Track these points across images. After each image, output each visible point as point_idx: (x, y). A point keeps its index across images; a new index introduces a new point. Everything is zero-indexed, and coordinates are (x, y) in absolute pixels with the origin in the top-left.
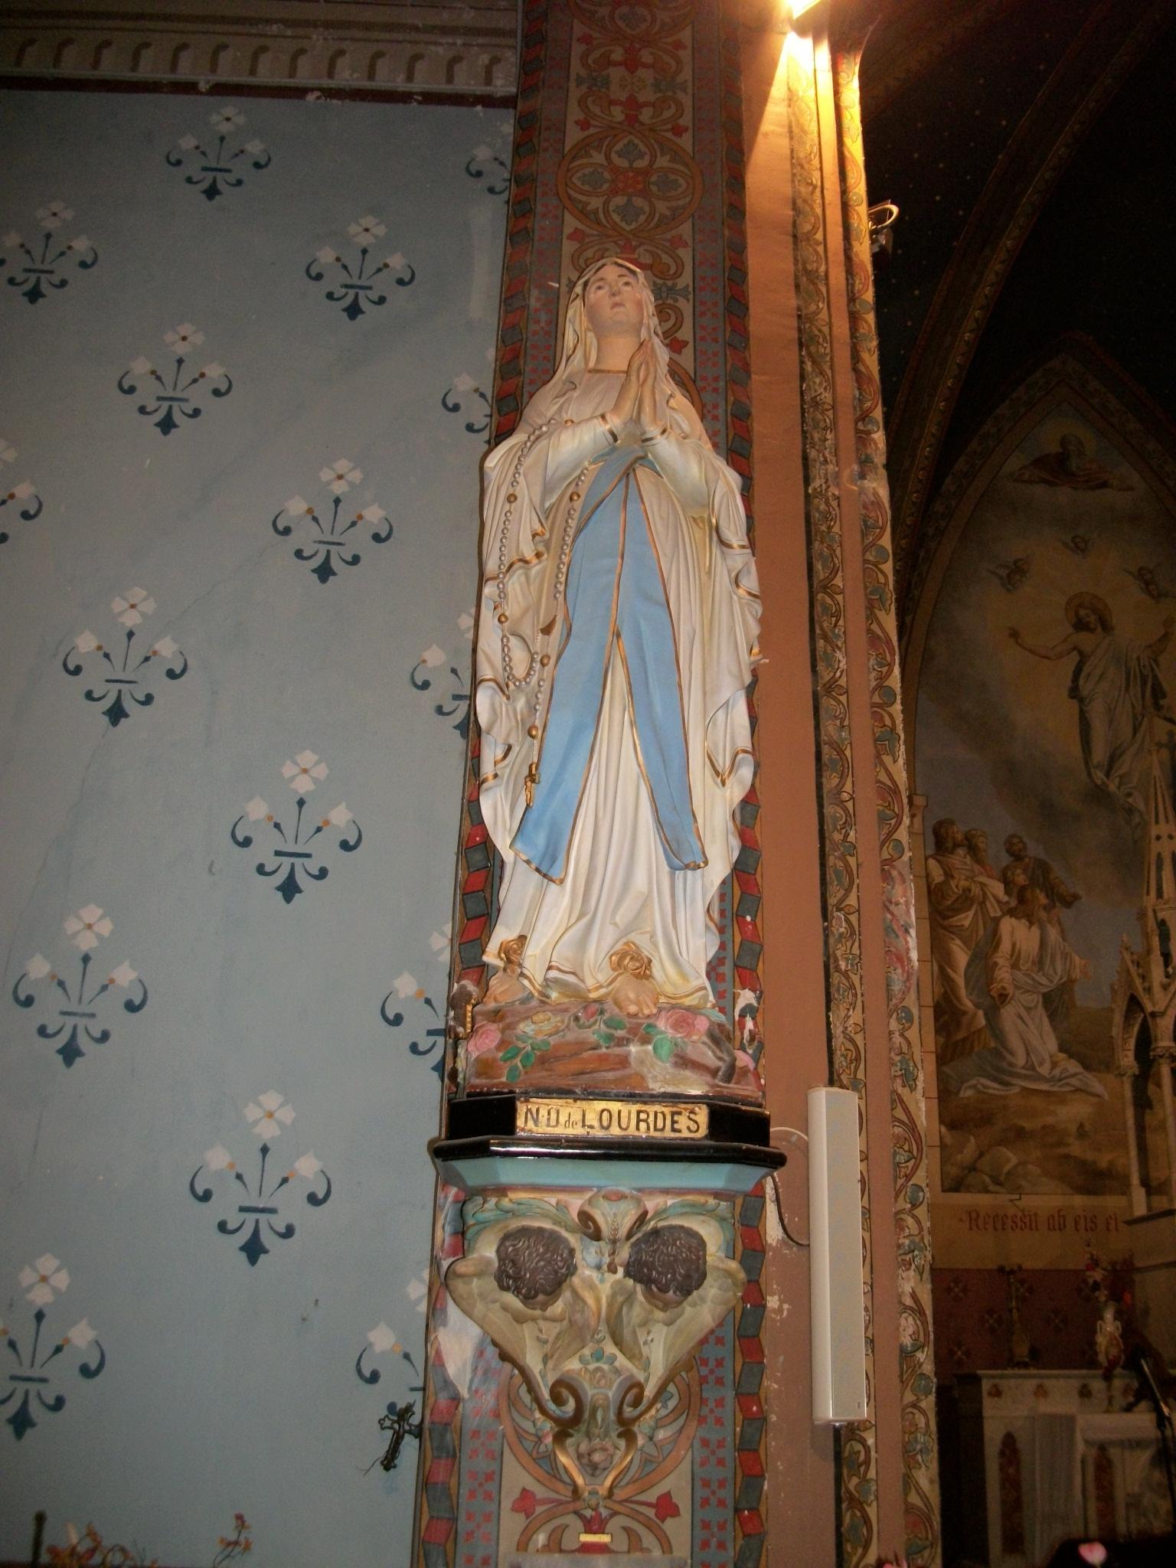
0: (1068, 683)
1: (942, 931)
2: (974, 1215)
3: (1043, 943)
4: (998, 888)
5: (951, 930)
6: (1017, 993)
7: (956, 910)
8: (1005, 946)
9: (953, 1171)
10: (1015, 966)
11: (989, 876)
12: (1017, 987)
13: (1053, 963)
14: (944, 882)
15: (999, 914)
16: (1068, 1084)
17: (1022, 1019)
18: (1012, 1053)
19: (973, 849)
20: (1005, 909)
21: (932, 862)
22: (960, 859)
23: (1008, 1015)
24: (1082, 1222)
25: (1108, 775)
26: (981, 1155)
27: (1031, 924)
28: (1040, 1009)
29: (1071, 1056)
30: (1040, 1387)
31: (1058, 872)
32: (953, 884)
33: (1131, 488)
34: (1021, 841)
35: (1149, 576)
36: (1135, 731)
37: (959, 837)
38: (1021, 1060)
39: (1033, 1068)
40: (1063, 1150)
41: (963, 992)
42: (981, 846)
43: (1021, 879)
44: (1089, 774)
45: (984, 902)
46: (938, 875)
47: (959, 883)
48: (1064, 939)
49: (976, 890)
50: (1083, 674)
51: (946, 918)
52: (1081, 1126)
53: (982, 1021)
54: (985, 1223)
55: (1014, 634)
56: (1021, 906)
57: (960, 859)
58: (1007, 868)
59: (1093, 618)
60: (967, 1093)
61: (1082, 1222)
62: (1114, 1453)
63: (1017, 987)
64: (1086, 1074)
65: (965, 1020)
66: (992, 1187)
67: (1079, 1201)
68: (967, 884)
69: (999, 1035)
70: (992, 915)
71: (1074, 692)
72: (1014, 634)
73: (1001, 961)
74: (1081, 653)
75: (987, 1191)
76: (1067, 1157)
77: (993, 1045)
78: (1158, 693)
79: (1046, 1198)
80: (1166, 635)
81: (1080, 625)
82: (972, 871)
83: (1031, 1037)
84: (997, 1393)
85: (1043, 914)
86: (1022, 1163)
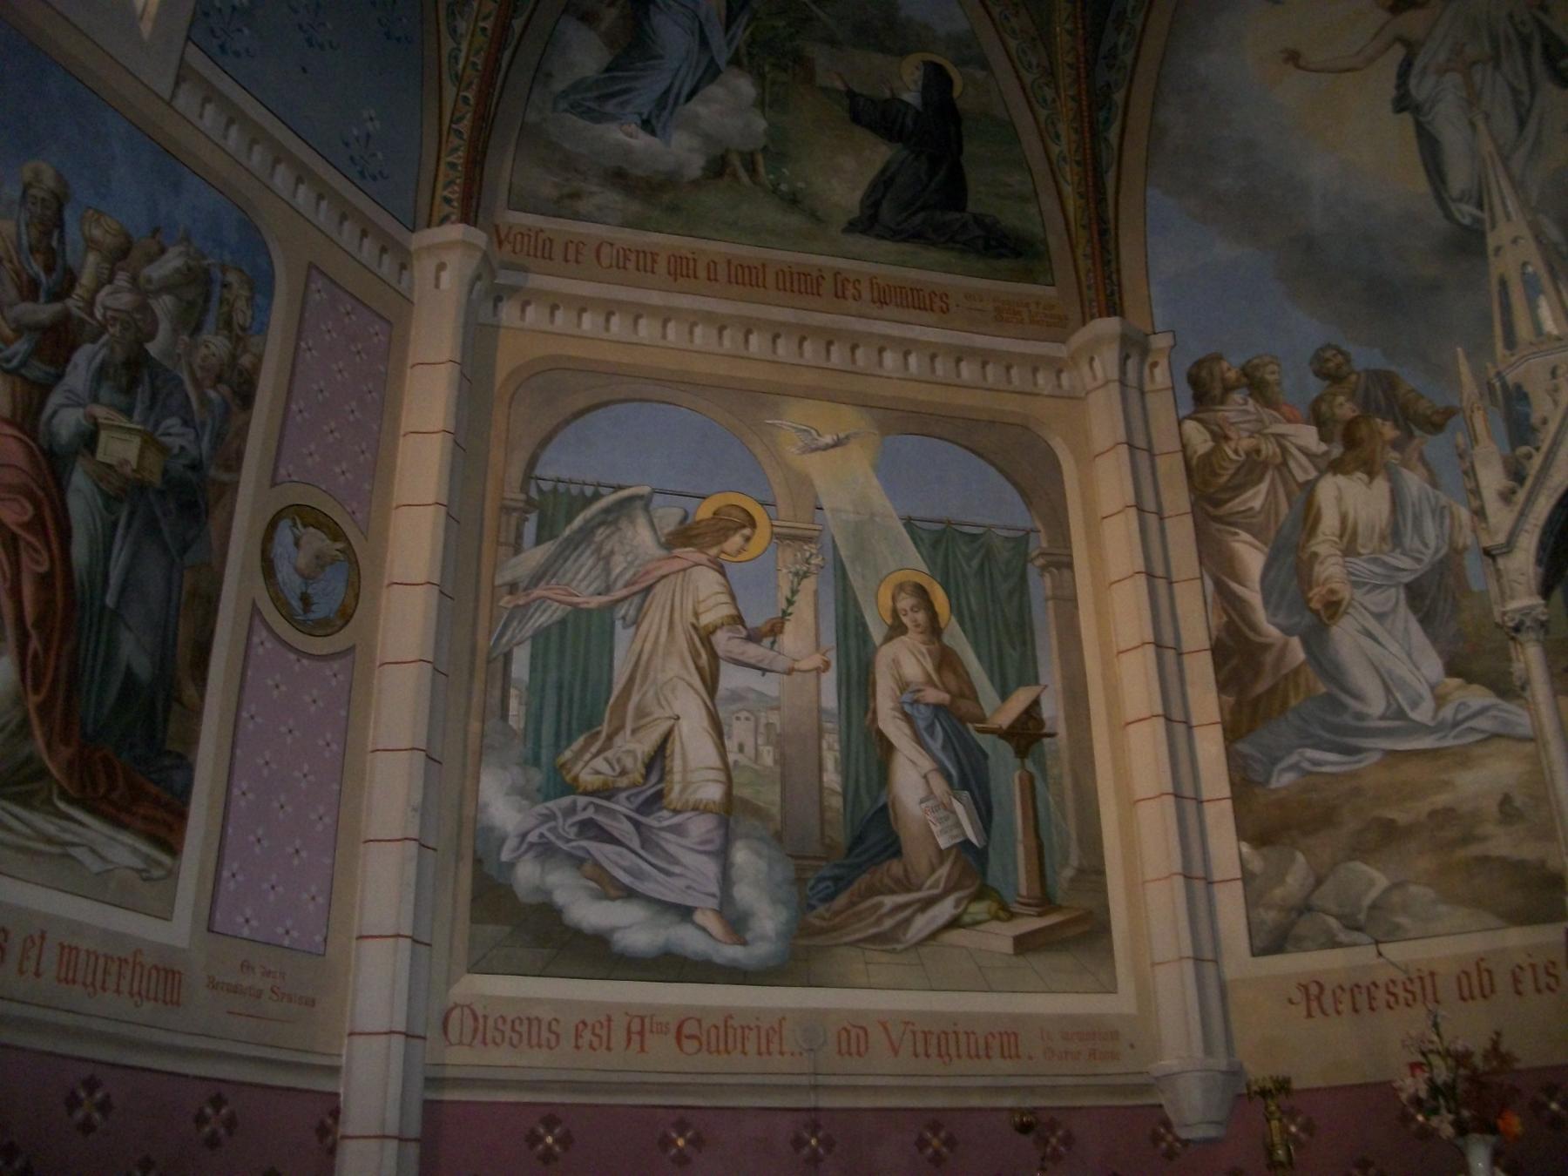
0: (1390, 91)
2: (1314, 990)
3: (1396, 499)
4: (1308, 436)
5: (1229, 521)
6: (1358, 594)
7: (1237, 489)
8: (1329, 522)
9: (1270, 916)
10: (1349, 551)
11: (1289, 421)
14: (1208, 455)
15: (1313, 474)
18: (1357, 697)
19: (1254, 384)
20: (1323, 465)
21: (1191, 427)
22: (1238, 409)
23: (1345, 637)
25: (1480, 206)
26: (1319, 882)
27: (1371, 475)
28: (1403, 610)
29: (1469, 678)
31: (1412, 379)
36: (1522, 123)
37: (1232, 375)
38: (1376, 704)
39: (1400, 714)
40: (1475, 850)
41: (1261, 615)
44: (1448, 215)
45: (1285, 463)
48: (1435, 485)
49: (1269, 449)
51: (1218, 504)
52: (1506, 800)
53: (1297, 652)
54: (1337, 1001)
56: (1352, 451)
57: (1238, 409)
60: (1283, 780)
63: (1355, 585)
65: (1269, 659)
66: (1343, 937)
67: (1516, 938)
68: (1253, 442)
69: (1331, 671)
70: (1301, 477)
71: (1403, 102)
72: (1293, 57)
76: (1484, 860)
77: (1322, 688)
79: (1447, 941)
82: (1261, 421)
85: (1393, 456)
86: (1396, 886)
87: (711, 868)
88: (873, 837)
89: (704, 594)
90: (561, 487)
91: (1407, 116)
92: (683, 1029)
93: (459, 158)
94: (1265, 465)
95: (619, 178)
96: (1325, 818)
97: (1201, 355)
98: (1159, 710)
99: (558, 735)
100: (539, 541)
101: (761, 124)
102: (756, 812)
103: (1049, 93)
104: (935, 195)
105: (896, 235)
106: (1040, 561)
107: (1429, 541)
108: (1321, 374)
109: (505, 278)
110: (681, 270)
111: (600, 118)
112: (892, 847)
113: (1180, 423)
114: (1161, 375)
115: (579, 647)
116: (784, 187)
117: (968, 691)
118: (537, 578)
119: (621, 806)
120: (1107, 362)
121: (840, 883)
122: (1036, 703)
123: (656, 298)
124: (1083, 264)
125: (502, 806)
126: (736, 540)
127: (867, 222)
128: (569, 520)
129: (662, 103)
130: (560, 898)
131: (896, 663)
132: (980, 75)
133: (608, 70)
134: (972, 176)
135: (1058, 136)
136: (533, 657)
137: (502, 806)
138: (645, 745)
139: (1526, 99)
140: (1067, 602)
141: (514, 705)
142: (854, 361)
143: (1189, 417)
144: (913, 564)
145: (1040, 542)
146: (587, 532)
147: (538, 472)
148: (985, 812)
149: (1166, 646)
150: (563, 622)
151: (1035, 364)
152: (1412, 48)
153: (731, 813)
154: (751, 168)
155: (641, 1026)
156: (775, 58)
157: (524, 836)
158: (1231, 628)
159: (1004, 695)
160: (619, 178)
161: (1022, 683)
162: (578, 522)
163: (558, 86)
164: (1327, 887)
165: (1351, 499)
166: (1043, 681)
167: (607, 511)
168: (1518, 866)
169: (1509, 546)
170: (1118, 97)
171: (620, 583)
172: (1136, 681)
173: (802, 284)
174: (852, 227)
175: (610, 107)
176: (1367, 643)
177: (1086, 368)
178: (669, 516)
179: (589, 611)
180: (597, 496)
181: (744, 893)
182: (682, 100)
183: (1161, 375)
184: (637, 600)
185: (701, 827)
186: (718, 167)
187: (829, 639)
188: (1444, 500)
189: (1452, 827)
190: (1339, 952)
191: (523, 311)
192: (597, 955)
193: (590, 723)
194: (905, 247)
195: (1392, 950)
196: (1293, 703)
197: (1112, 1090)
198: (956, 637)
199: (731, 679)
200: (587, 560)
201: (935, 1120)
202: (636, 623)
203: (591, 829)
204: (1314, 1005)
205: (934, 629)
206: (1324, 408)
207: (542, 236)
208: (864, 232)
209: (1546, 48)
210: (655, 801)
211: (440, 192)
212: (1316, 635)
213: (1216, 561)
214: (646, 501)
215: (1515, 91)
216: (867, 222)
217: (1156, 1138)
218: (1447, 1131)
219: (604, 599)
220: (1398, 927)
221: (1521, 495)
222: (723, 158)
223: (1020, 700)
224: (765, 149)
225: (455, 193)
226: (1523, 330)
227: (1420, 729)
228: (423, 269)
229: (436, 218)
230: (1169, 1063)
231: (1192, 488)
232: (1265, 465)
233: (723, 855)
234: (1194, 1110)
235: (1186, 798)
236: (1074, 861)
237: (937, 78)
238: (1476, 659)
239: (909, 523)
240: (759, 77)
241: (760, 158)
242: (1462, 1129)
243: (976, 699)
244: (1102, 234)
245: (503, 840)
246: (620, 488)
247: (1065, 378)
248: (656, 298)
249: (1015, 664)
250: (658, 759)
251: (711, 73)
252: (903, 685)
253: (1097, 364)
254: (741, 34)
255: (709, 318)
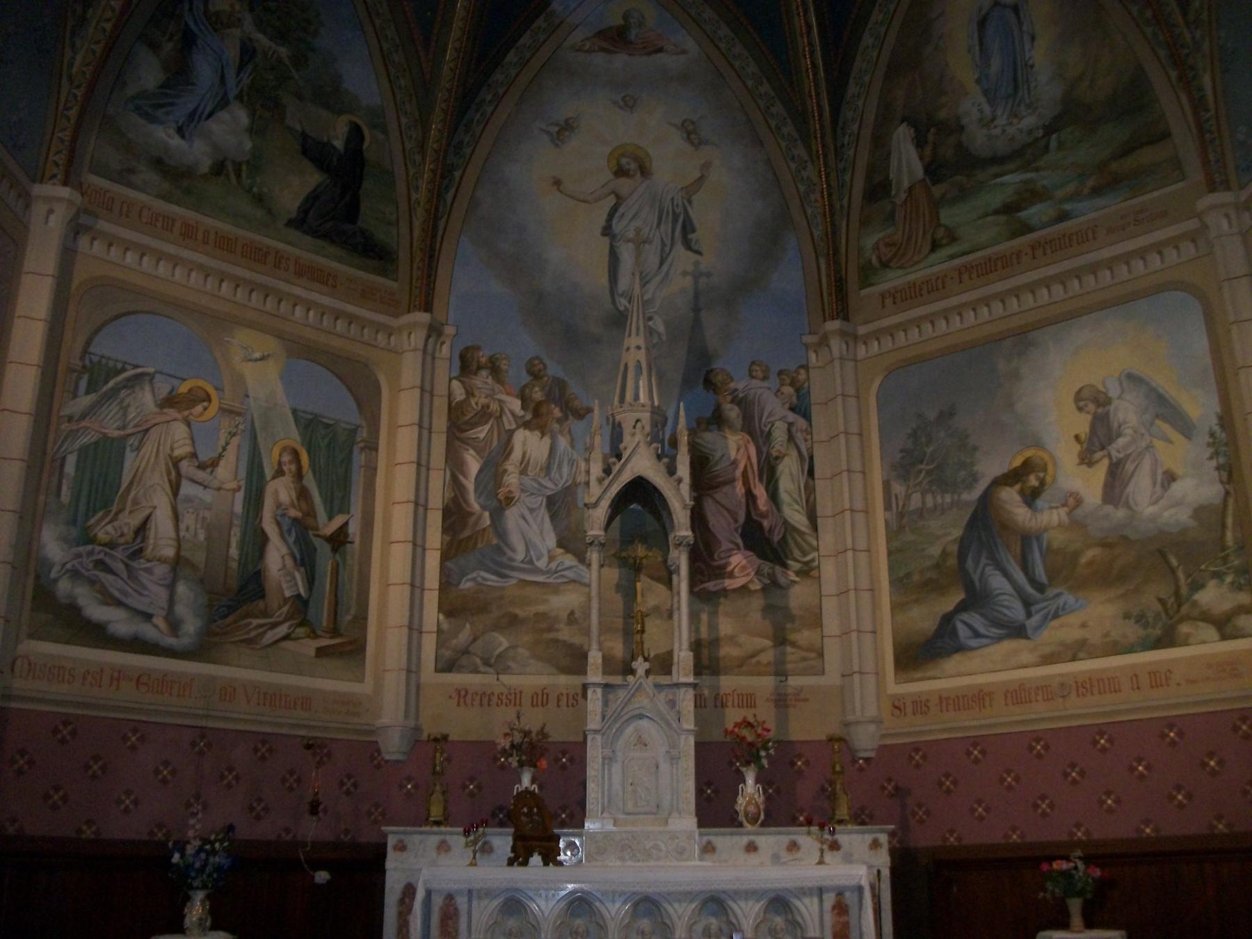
0: (601, 221)
1: (457, 443)
2: (463, 693)
3: (552, 449)
4: (515, 404)
7: (473, 425)
8: (516, 455)
9: (448, 654)
10: (523, 472)
11: (508, 394)
12: (523, 491)
13: (560, 467)
14: (462, 402)
15: (514, 426)
16: (563, 576)
17: (524, 518)
18: (513, 550)
19: (495, 370)
21: (455, 383)
22: (483, 380)
23: (512, 516)
24: (564, 699)
26: (475, 640)
27: (543, 435)
30: (443, 842)
31: (574, 388)
32: (473, 402)
33: (684, 52)
34: (542, 362)
35: (691, 127)
36: (661, 263)
37: (483, 360)
38: (520, 556)
39: (531, 562)
41: (472, 497)
42: (504, 367)
43: (538, 395)
44: (614, 302)
45: (501, 416)
46: (459, 393)
47: (480, 400)
48: (573, 447)
49: (494, 407)
50: (617, 215)
52: (572, 613)
53: (486, 520)
54: (473, 700)
55: (557, 183)
56: (536, 419)
57: (483, 380)
58: (525, 386)
59: (633, 166)
60: (466, 585)
61: (564, 699)
62: (462, 902)
63: (523, 491)
64: (581, 567)
65: (472, 520)
66: (482, 669)
69: (502, 534)
70: (507, 427)
71: (607, 231)
72: (557, 183)
73: (510, 468)
74: (618, 197)
75: (478, 672)
76: (556, 641)
77: (495, 541)
78: (688, 227)
79: (532, 677)
80: (701, 179)
81: (621, 172)
82: (493, 390)
83: (531, 533)
84: (401, 847)
85: (556, 426)
87: (163, 594)
88: (251, 586)
89: (178, 437)
90: (104, 361)
91: (607, 240)
92: (140, 679)
93: (66, 136)
94: (491, 415)
95: (159, 164)
96: (483, 608)
97: (470, 344)
98: (411, 538)
99: (88, 509)
100: (87, 393)
101: (248, 145)
102: (193, 567)
103: (418, 158)
104: (343, 215)
105: (315, 234)
106: (362, 445)
107: (563, 476)
108: (530, 372)
109: (83, 220)
110: (188, 233)
111: (152, 119)
112: (261, 593)
113: (450, 380)
114: (445, 350)
115: (104, 460)
116: (255, 189)
117: (311, 513)
118: (83, 416)
119: (118, 553)
120: (418, 338)
121: (231, 609)
122: (346, 524)
123: (171, 249)
124: (416, 273)
125: (53, 546)
126: (199, 408)
127: (298, 222)
128: (106, 382)
129: (192, 116)
130: (81, 601)
131: (276, 492)
132: (381, 137)
133: (162, 87)
134: (365, 206)
135: (417, 188)
136: (78, 462)
137: (53, 546)
138: (136, 521)
139: (667, 249)
140: (372, 470)
141: (64, 488)
142: (278, 309)
143: (455, 378)
144: (293, 436)
145: (363, 434)
146: (115, 391)
147: (92, 349)
148: (311, 581)
149: (420, 505)
150: (96, 443)
151: (379, 328)
152: (620, 199)
153: (178, 563)
154: (239, 176)
155: (119, 675)
156: (263, 101)
157: (64, 565)
158: (455, 500)
159: (330, 518)
160: (159, 164)
161: (341, 511)
162: (111, 384)
163: (131, 91)
164: (479, 642)
165: (530, 445)
166: (352, 511)
167: (128, 380)
168: (570, 646)
169: (595, 505)
170: (457, 174)
171: (131, 425)
172: (401, 521)
173: (257, 255)
174: (290, 223)
175: (160, 113)
176: (522, 522)
177: (405, 336)
178: (163, 388)
179: (113, 439)
180: (123, 370)
181: (181, 610)
182: (204, 116)
183: (445, 350)
184: (140, 436)
185: (161, 570)
186: (219, 169)
187: (243, 474)
188: (575, 457)
189: (546, 622)
190: (479, 676)
191: (92, 244)
192: (98, 635)
193: (106, 505)
194: (320, 242)
195: (503, 678)
196: (479, 546)
197: (356, 731)
198: (310, 481)
199: (187, 489)
200: (114, 407)
201: (264, 738)
202: (138, 449)
203: (101, 565)
204: (462, 701)
205: (299, 476)
206: (527, 390)
207: (108, 195)
208: (297, 228)
209: (684, 222)
210: (138, 554)
211: (51, 158)
212: (497, 514)
213: (454, 462)
214: (151, 377)
215: (663, 244)
216: (298, 222)
217: (372, 758)
218: (515, 764)
219: (122, 433)
220: (509, 667)
221: (606, 482)
222: (223, 162)
223: (338, 521)
224: (248, 162)
225: (61, 159)
226: (629, 396)
227: (537, 571)
228: (39, 209)
229: (47, 175)
230: (385, 721)
231: (449, 419)
232: (491, 415)
233: (171, 587)
234: (393, 746)
235: (416, 586)
236: (353, 611)
237: (356, 133)
238: (571, 542)
239: (294, 412)
240: (252, 114)
241: (244, 168)
242: (521, 764)
243: (315, 517)
244: (431, 257)
245: (51, 566)
246: (136, 367)
247: (393, 338)
248: (171, 249)
249: (338, 500)
250: (142, 529)
251: (223, 103)
252: (279, 505)
253: (413, 336)
254: (246, 81)
255: (201, 267)
